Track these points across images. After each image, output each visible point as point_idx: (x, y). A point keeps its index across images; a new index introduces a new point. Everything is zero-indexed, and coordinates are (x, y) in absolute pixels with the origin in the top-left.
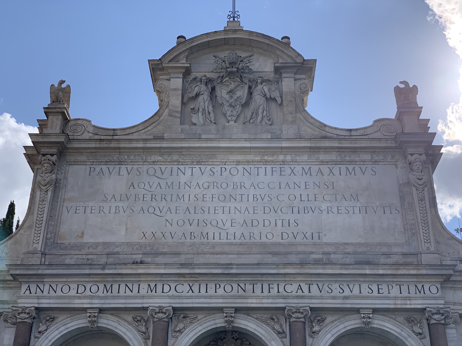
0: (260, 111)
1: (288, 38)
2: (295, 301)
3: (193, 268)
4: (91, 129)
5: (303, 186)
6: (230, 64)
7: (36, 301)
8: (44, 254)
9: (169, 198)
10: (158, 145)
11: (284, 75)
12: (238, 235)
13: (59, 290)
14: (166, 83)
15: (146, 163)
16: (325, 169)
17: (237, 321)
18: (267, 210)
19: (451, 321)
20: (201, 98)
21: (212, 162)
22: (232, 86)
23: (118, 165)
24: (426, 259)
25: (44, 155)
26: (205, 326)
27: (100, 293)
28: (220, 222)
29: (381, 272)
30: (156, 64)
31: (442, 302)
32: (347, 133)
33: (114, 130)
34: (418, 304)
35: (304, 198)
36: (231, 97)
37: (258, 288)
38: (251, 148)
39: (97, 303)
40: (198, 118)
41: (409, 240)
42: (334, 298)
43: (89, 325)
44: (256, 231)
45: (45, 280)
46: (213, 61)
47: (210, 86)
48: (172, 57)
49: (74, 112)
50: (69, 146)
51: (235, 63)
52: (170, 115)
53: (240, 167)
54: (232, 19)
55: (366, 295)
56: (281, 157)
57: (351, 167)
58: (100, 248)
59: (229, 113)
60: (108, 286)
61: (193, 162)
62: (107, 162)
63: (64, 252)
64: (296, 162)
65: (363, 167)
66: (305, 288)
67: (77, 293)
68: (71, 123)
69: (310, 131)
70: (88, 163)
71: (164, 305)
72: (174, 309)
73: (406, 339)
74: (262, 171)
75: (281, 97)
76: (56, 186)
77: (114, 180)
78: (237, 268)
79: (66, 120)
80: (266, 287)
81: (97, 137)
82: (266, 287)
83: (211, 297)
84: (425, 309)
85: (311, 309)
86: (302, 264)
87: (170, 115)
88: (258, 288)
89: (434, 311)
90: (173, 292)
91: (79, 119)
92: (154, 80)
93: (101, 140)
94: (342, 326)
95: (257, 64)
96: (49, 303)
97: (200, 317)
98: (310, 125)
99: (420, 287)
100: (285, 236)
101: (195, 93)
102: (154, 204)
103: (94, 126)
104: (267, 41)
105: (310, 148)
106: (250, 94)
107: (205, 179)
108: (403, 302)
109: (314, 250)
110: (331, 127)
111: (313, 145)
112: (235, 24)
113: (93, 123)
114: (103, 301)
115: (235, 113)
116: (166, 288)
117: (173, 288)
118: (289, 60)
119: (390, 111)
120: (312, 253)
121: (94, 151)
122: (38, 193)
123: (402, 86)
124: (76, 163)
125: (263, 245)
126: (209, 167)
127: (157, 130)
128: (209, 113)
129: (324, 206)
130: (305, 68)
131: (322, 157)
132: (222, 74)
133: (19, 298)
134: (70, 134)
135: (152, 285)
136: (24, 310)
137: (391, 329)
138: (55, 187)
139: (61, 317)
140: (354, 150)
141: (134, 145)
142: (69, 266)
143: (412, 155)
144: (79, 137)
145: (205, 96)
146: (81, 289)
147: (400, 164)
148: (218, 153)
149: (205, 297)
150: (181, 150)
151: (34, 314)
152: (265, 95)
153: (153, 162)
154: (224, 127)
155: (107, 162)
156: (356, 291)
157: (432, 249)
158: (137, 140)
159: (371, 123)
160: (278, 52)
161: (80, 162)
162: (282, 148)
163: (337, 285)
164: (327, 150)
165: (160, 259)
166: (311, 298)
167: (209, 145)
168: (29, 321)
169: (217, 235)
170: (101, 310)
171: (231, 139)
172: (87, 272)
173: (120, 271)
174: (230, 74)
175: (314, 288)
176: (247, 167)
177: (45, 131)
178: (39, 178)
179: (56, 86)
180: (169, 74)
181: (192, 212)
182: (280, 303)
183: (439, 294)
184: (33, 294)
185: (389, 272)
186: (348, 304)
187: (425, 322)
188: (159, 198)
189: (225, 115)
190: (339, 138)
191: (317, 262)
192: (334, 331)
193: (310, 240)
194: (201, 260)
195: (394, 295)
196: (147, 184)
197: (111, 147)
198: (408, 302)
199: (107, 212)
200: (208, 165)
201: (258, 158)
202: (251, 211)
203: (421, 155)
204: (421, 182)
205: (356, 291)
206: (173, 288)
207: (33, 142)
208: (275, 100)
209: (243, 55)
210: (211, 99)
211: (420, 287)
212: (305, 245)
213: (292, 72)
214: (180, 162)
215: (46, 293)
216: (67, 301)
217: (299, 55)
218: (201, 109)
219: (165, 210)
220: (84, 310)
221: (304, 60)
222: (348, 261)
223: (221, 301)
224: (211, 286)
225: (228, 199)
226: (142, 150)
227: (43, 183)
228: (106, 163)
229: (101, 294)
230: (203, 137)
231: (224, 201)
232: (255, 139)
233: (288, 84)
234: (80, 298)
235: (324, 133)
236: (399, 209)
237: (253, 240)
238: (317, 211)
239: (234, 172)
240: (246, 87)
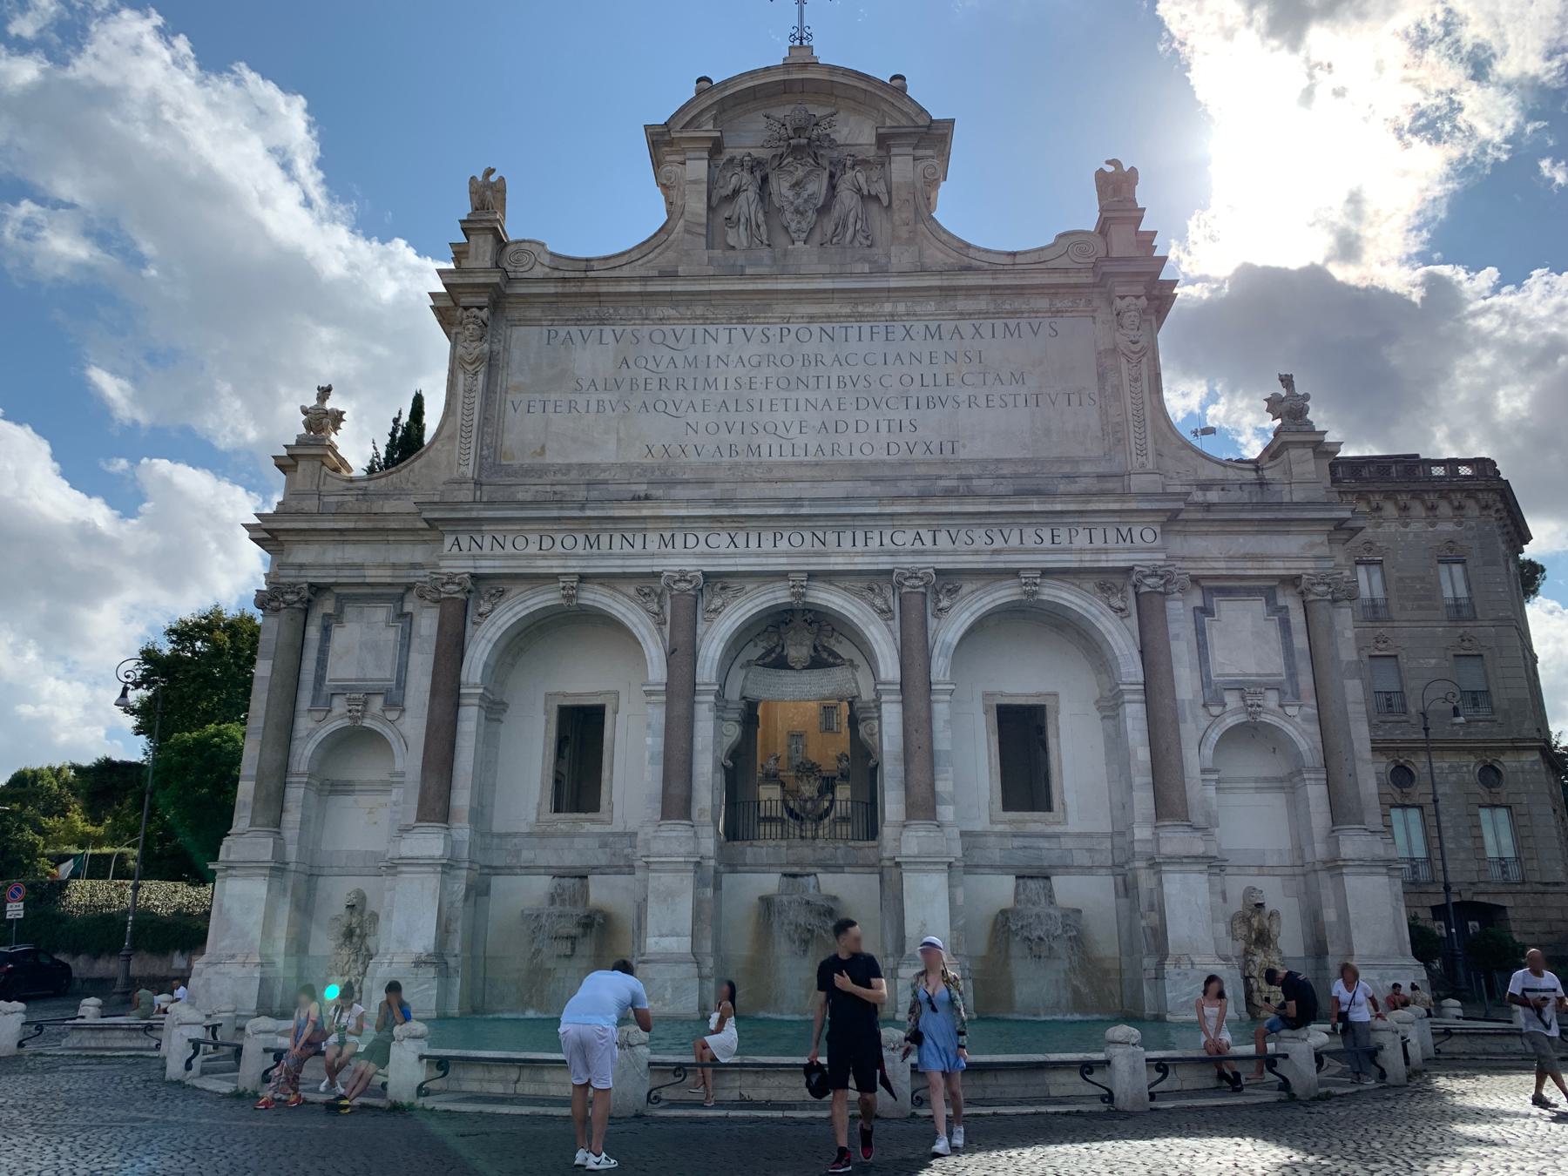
0: (851, 220)
1: (902, 78)
2: (910, 559)
4: (546, 260)
5: (926, 360)
6: (795, 130)
7: (471, 563)
8: (478, 484)
9: (690, 384)
10: (668, 289)
11: (894, 151)
12: (812, 449)
13: (509, 545)
14: (678, 169)
16: (966, 326)
17: (811, 593)
18: (862, 403)
19: (1175, 588)
20: (743, 196)
22: (800, 173)
24: (1137, 483)
25: (466, 308)
26: (757, 602)
27: (579, 550)
29: (1059, 507)
30: (658, 134)
31: (1163, 556)
32: (1008, 260)
33: (587, 260)
34: (1119, 560)
35: (928, 380)
36: (798, 195)
37: (847, 538)
38: (833, 291)
39: (575, 566)
40: (739, 237)
42: (977, 553)
43: (563, 601)
44: (843, 442)
46: (762, 126)
47: (758, 175)
48: (688, 118)
49: (513, 230)
50: (508, 291)
51: (804, 129)
52: (687, 231)
53: (815, 328)
54: (797, 43)
55: (1030, 547)
56: (888, 308)
57: (1012, 323)
58: (574, 475)
59: (793, 226)
60: (593, 538)
63: (513, 480)
65: (1035, 323)
66: (927, 537)
68: (510, 249)
69: (940, 256)
72: (704, 574)
74: (853, 333)
75: (889, 193)
76: (492, 364)
77: (592, 352)
79: (501, 243)
80: (860, 536)
81: (557, 274)
82: (860, 536)
83: (767, 555)
84: (1132, 568)
85: (938, 572)
86: (923, 497)
87: (687, 231)
88: (847, 538)
89: (1148, 572)
90: (702, 547)
92: (657, 164)
93: (565, 279)
94: (988, 599)
95: (845, 131)
97: (749, 587)
98: (940, 245)
99: (1124, 531)
100: (894, 449)
101: (731, 187)
102: (664, 395)
103: (551, 254)
104: (863, 85)
105: (940, 288)
106: (833, 187)
107: (754, 349)
108: (1094, 557)
109: (944, 472)
110: (979, 249)
111: (946, 283)
112: (805, 52)
113: (550, 248)
114: (584, 563)
115: (804, 225)
116: (691, 541)
117: (702, 540)
118: (904, 122)
119: (1087, 217)
120: (940, 478)
122: (461, 377)
123: (1110, 169)
124: (524, 322)
125: (856, 465)
126: (760, 328)
127: (667, 259)
128: (758, 226)
129: (963, 396)
130: (933, 136)
131: (963, 304)
132: (780, 151)
133: (442, 558)
134: (509, 268)
135: (667, 536)
136: (451, 579)
138: (490, 365)
139: (516, 590)
140: (1019, 291)
141: (624, 288)
142: (522, 504)
143: (1122, 298)
144: (526, 275)
145: (751, 193)
146: (547, 543)
149: (758, 555)
151: (469, 585)
152: (860, 190)
154: (785, 254)
156: (1014, 541)
157: (1150, 466)
158: (631, 279)
159: (1051, 241)
160: (885, 107)
162: (889, 290)
163: (982, 531)
164: (970, 291)
165: (679, 492)
166: (938, 553)
167: (760, 287)
168: (461, 596)
169: (776, 449)
170: (583, 578)
171: (799, 276)
172: (555, 513)
173: (611, 513)
174: (796, 150)
175: (943, 538)
176: (828, 327)
177: (465, 264)
178: (460, 351)
180: (683, 151)
181: (732, 408)
182: (884, 563)
183: (1158, 542)
184: (465, 552)
185: (1072, 507)
186: (1000, 562)
187: (1130, 590)
189: (786, 229)
190: (995, 270)
191: (949, 494)
192: (975, 607)
193: (937, 456)
194: (748, 492)
195: (1080, 546)
196: (650, 360)
197: (584, 292)
198: (1103, 557)
201: (847, 310)
202: (834, 405)
203: (1138, 297)
204: (1136, 348)
205: (1014, 541)
206: (702, 540)
207: (445, 285)
208: (877, 198)
209: (819, 112)
210: (762, 199)
211: (1124, 531)
212: (928, 464)
213: (909, 145)
215: (487, 550)
216: (524, 563)
217: (923, 110)
218: (743, 220)
219: (684, 406)
220: (555, 577)
222: (1002, 489)
223: (784, 560)
224: (768, 538)
225: (793, 385)
227: (468, 358)
228: (577, 321)
229: (581, 552)
230: (748, 271)
231: (787, 389)
232: (840, 275)
233: (902, 168)
234: (544, 557)
235: (966, 258)
236: (1096, 398)
237: (837, 457)
238: (950, 402)
239: (804, 335)
240: (826, 175)
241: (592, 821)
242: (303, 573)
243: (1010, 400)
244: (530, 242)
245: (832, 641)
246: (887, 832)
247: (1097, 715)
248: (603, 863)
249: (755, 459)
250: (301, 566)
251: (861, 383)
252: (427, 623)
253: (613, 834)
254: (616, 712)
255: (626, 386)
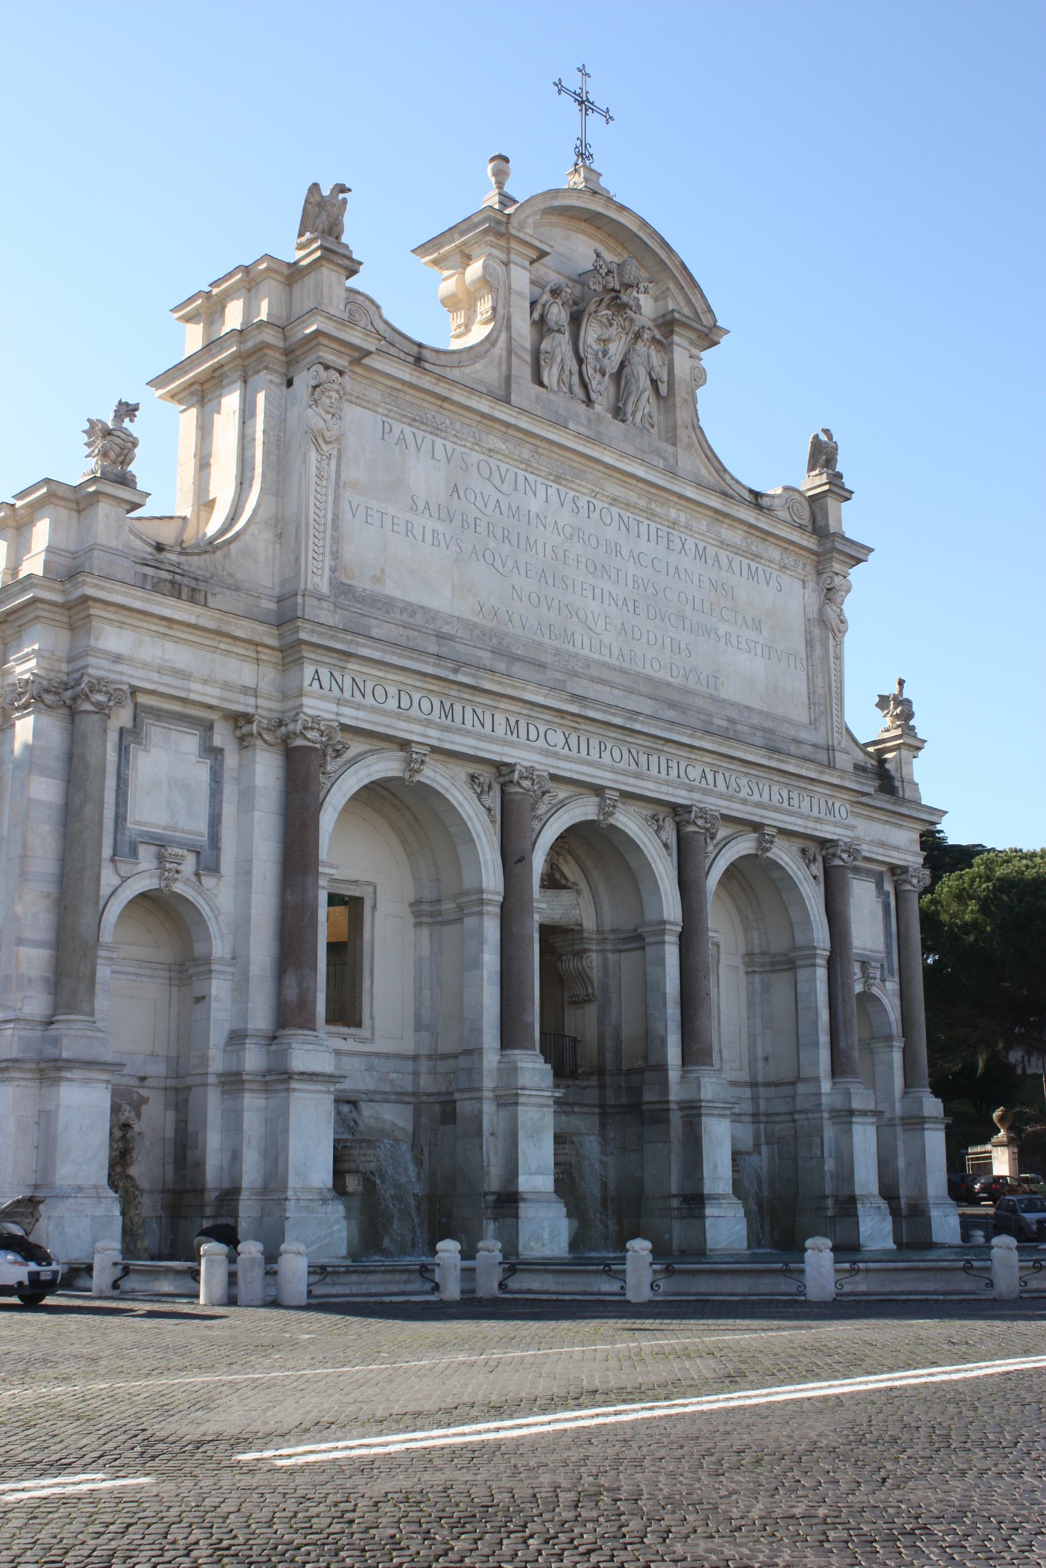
3: (585, 707)
7: (333, 707)
12: (616, 652)
15: (477, 448)
21: (579, 485)
23: (431, 433)
28: (590, 615)
33: (420, 345)
34: (826, 831)
39: (434, 737)
41: (815, 719)
45: (350, 666)
53: (615, 510)
56: (673, 513)
57: (754, 565)
59: (594, 384)
61: (550, 474)
62: (414, 420)
64: (691, 530)
66: (710, 776)
67: (399, 707)
69: (707, 474)
70: (380, 410)
71: (537, 766)
73: (801, 882)
78: (642, 722)
91: (359, 293)
96: (357, 719)
104: (663, 255)
105: (717, 511)
107: (565, 517)
110: (733, 478)
118: (686, 310)
121: (399, 386)
123: (823, 438)
125: (649, 679)
126: (572, 494)
137: (787, 864)
147: (811, 584)
148: (590, 470)
150: (538, 443)
153: (490, 450)
155: (414, 420)
161: (369, 402)
162: (681, 497)
176: (625, 515)
179: (326, 192)
182: (680, 797)
184: (326, 691)
185: (812, 775)
188: (499, 533)
199: (420, 538)
200: (570, 488)
201: (642, 503)
214: (530, 466)
217: (710, 310)
221: (715, 325)
223: (609, 775)
225: (598, 572)
226: (478, 418)
230: (571, 425)
238: (713, 635)
241: (354, 1037)
242: (118, 667)
243: (752, 645)
244: (372, 301)
245: (561, 859)
246: (674, 1075)
247: (742, 969)
248: (371, 1086)
249: (570, 648)
250: (118, 659)
251: (650, 590)
252: (266, 769)
253: (378, 1055)
254: (374, 907)
255: (457, 521)
